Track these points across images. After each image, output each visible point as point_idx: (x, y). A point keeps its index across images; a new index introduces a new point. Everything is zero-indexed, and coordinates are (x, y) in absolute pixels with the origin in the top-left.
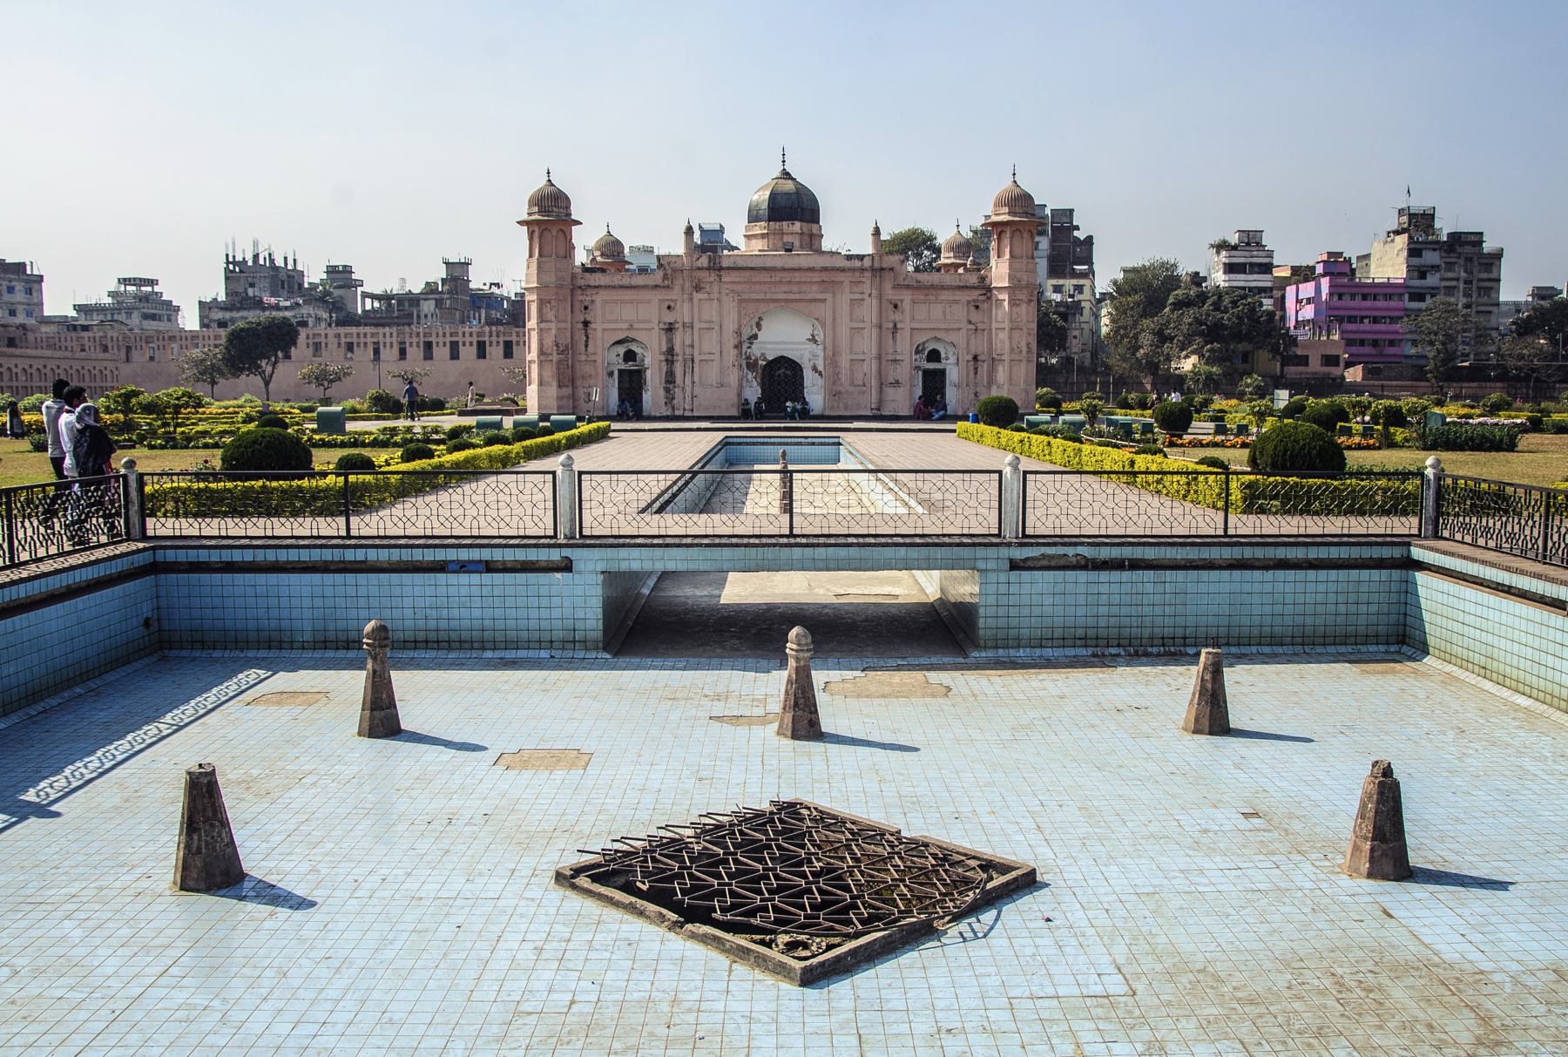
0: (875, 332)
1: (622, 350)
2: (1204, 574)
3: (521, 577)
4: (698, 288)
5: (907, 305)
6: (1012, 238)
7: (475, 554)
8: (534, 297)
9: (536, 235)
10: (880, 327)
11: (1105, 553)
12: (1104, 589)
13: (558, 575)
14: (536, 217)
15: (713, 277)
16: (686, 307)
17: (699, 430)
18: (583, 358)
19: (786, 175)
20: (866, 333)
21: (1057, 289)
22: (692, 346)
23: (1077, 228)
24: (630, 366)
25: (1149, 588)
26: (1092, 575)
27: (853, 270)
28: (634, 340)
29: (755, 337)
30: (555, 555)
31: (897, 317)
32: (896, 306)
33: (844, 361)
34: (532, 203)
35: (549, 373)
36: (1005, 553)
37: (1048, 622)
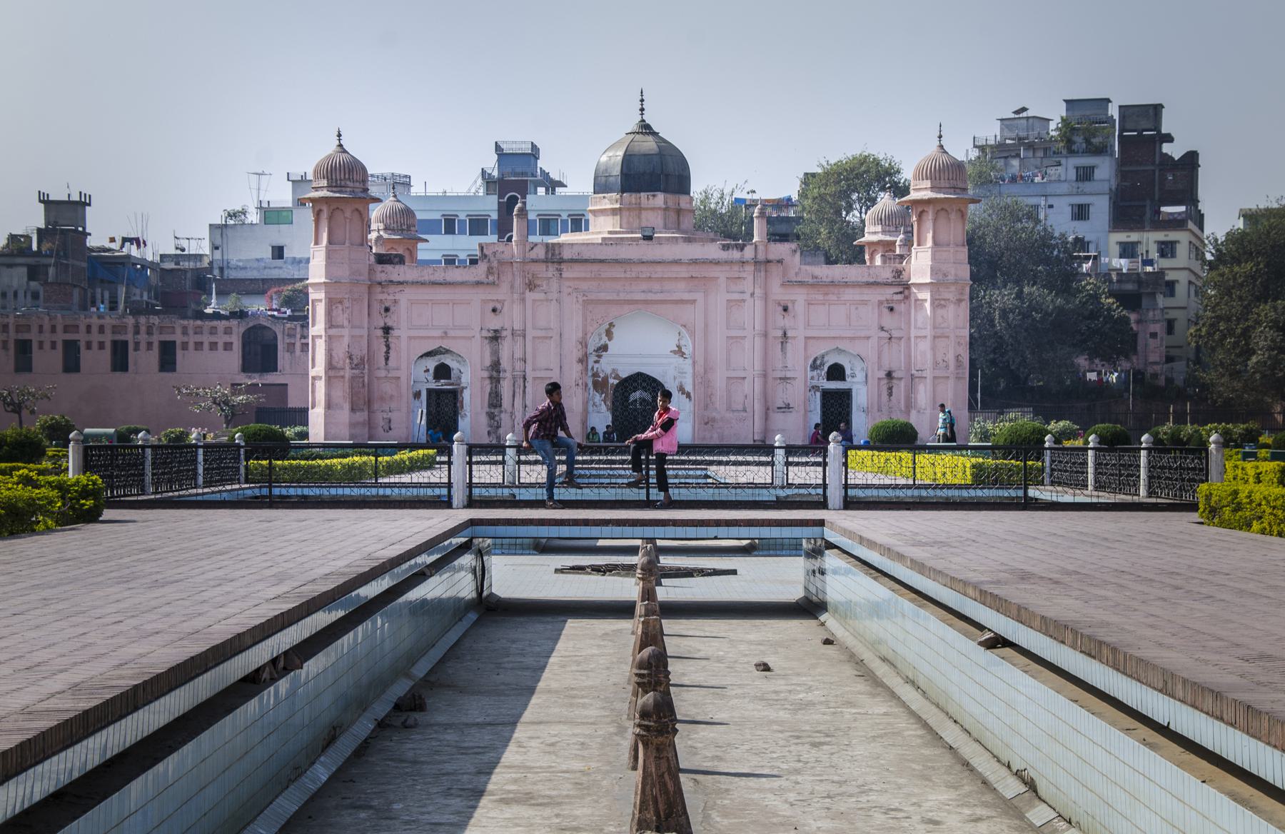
0: (758, 342)
1: (432, 364)
4: (531, 286)
5: (799, 308)
6: (935, 220)
8: (321, 295)
9: (325, 216)
10: (765, 335)
15: (552, 270)
16: (517, 308)
18: (382, 373)
20: (747, 344)
24: (442, 385)
27: (730, 263)
28: (447, 351)
29: (605, 348)
31: (787, 322)
32: (785, 309)
35: (341, 392)
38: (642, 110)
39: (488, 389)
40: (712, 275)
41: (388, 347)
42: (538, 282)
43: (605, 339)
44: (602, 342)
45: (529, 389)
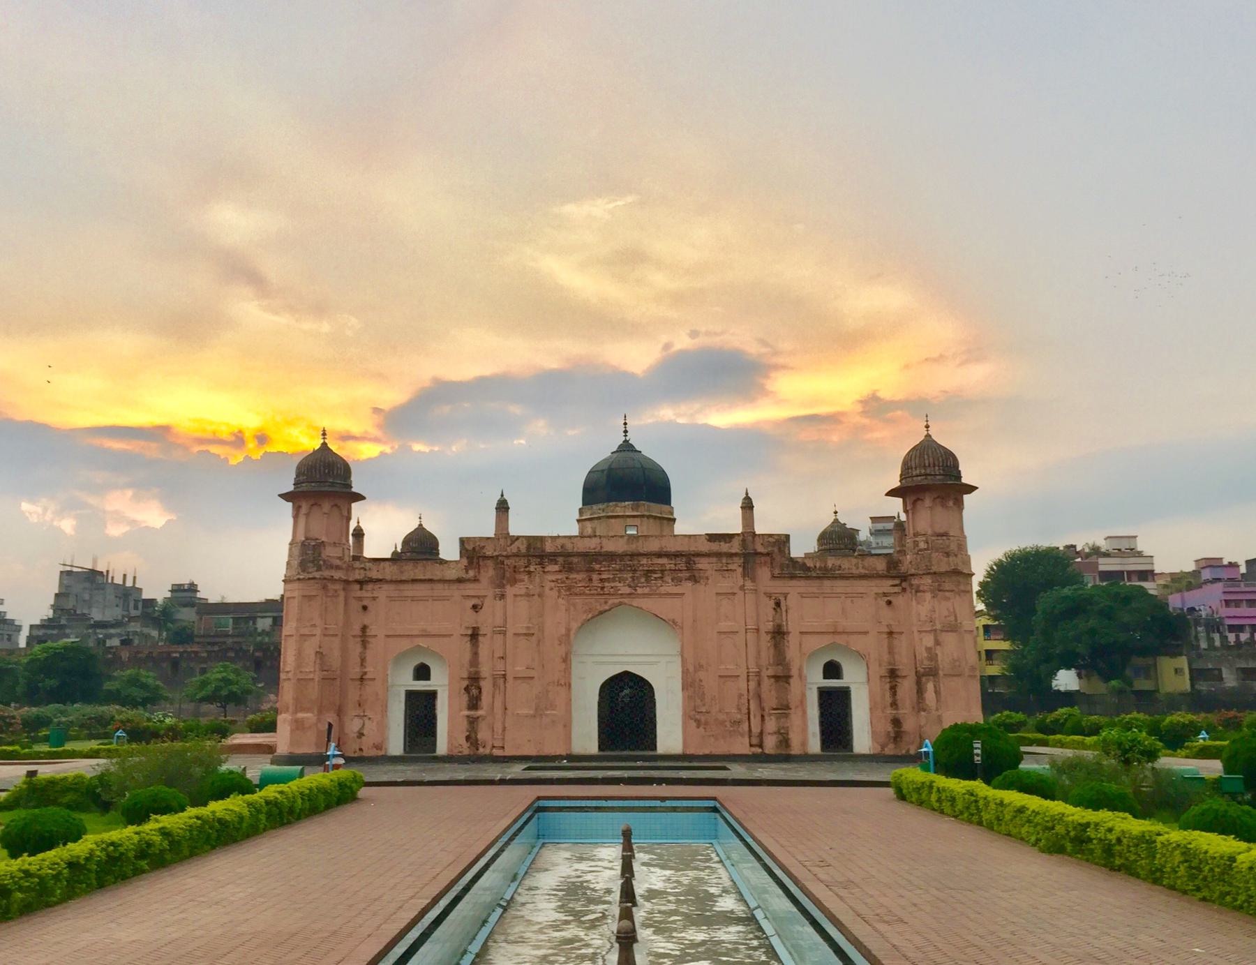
0: (751, 636)
5: (792, 601)
10: (758, 630)
17: (502, 782)
19: (626, 447)
24: (421, 685)
27: (719, 555)
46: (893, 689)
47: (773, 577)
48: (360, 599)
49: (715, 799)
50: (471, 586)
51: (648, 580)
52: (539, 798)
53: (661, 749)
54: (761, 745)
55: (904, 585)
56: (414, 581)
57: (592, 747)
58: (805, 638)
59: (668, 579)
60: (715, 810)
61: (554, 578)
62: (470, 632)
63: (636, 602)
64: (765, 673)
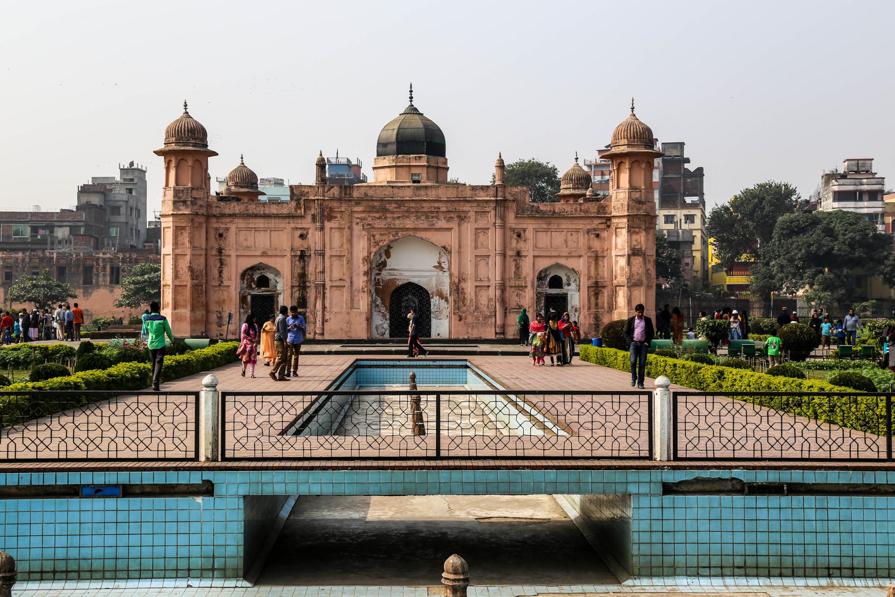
0: (498, 259)
2: (870, 500)
3: (159, 502)
5: (529, 234)
6: (630, 170)
7: (111, 478)
9: (173, 164)
11: (762, 477)
12: (762, 514)
13: (199, 500)
14: (173, 147)
16: (318, 234)
17: (329, 353)
19: (413, 111)
21: (669, 219)
22: (323, 272)
23: (688, 161)
25: (811, 514)
26: (750, 500)
29: (384, 264)
30: (196, 478)
31: (522, 245)
32: (519, 236)
33: (469, 288)
34: (168, 134)
36: (656, 476)
37: (704, 549)
38: (411, 98)
39: (297, 295)
40: (465, 209)
41: (222, 264)
42: (335, 215)
43: (384, 257)
44: (382, 260)
45: (327, 295)
46: (597, 295)
47: (516, 217)
48: (216, 229)
49: (466, 360)
50: (300, 221)
51: (427, 217)
52: (357, 360)
53: (434, 336)
54: (503, 333)
55: (608, 223)
56: (256, 216)
57: (387, 336)
58: (537, 260)
59: (442, 216)
60: (467, 367)
61: (359, 216)
62: (299, 253)
63: (419, 234)
64: (508, 284)
